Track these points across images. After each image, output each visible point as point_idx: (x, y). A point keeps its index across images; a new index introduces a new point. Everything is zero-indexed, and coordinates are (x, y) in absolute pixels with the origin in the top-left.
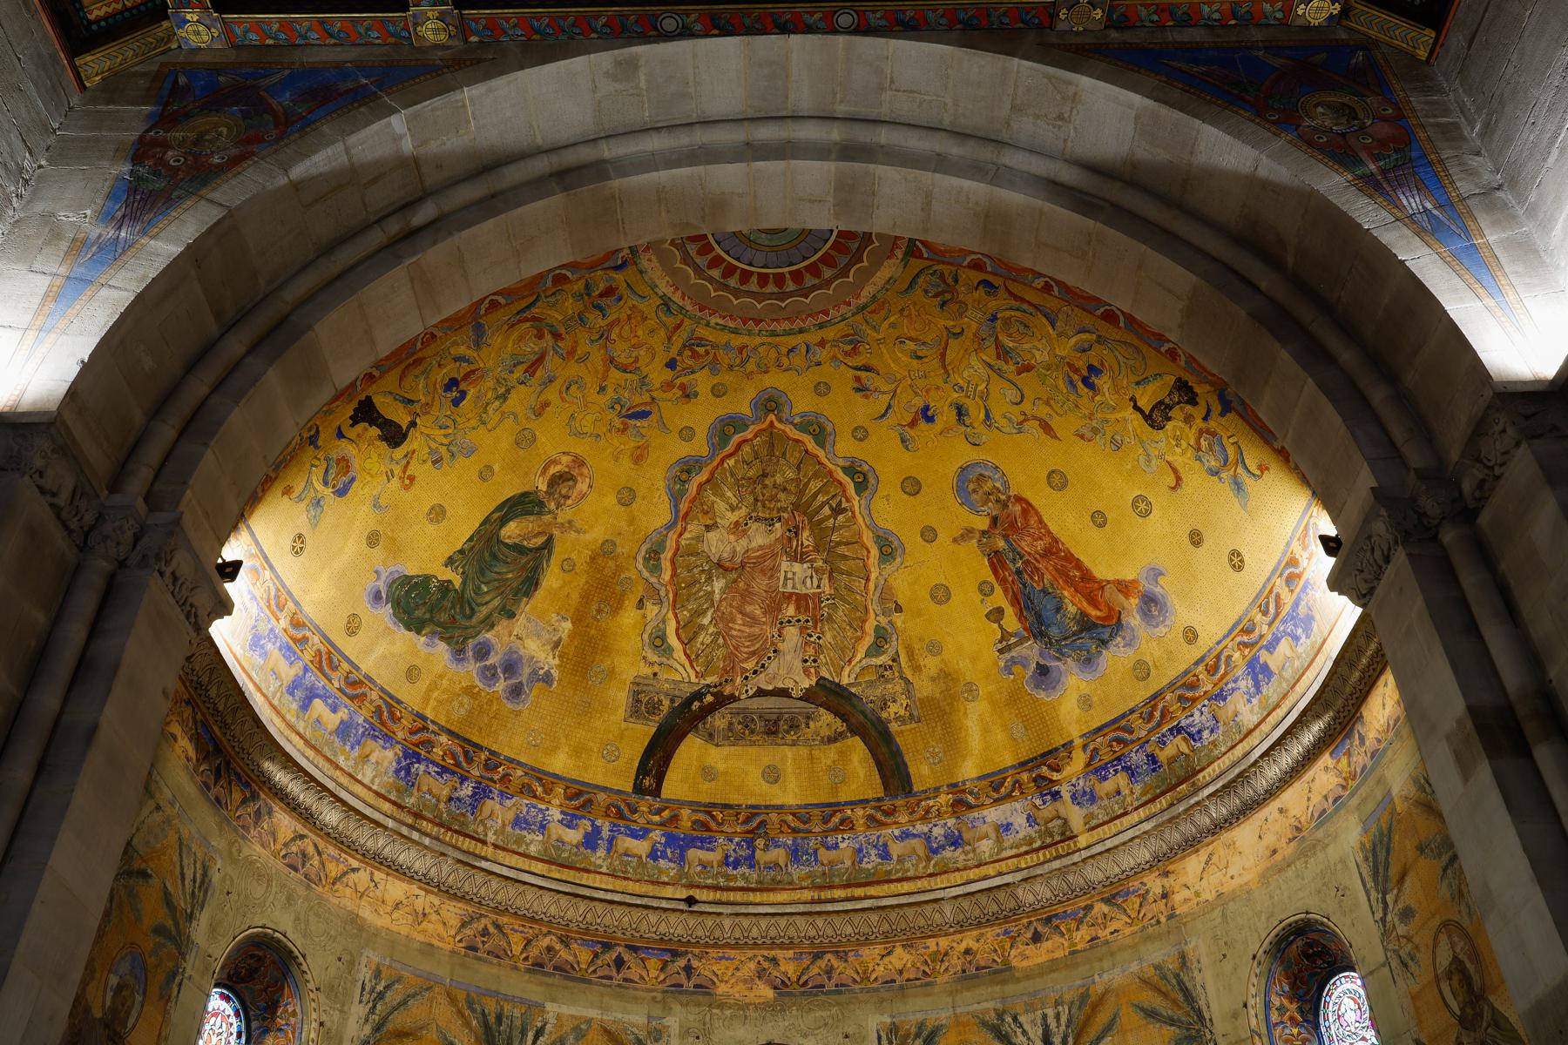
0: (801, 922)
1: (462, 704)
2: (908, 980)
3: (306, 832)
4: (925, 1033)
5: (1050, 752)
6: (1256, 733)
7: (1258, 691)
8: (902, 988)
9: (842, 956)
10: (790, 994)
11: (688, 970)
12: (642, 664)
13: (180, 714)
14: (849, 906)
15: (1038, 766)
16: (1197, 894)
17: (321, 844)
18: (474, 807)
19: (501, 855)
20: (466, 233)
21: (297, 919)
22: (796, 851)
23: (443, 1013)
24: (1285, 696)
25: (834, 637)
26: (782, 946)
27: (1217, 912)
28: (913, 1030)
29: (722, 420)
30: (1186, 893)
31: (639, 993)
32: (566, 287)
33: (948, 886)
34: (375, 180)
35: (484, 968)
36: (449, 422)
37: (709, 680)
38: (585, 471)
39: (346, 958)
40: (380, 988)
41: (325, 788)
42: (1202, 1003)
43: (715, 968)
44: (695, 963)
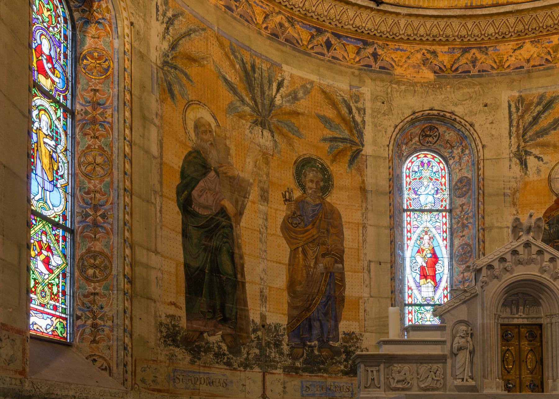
2: (533, 66)
4: (545, 102)
8: (528, 72)
9: (484, 50)
10: (445, 77)
11: (375, 55)
26: (440, 43)
28: (536, 100)
31: (343, 68)
43: (393, 56)
44: (380, 52)
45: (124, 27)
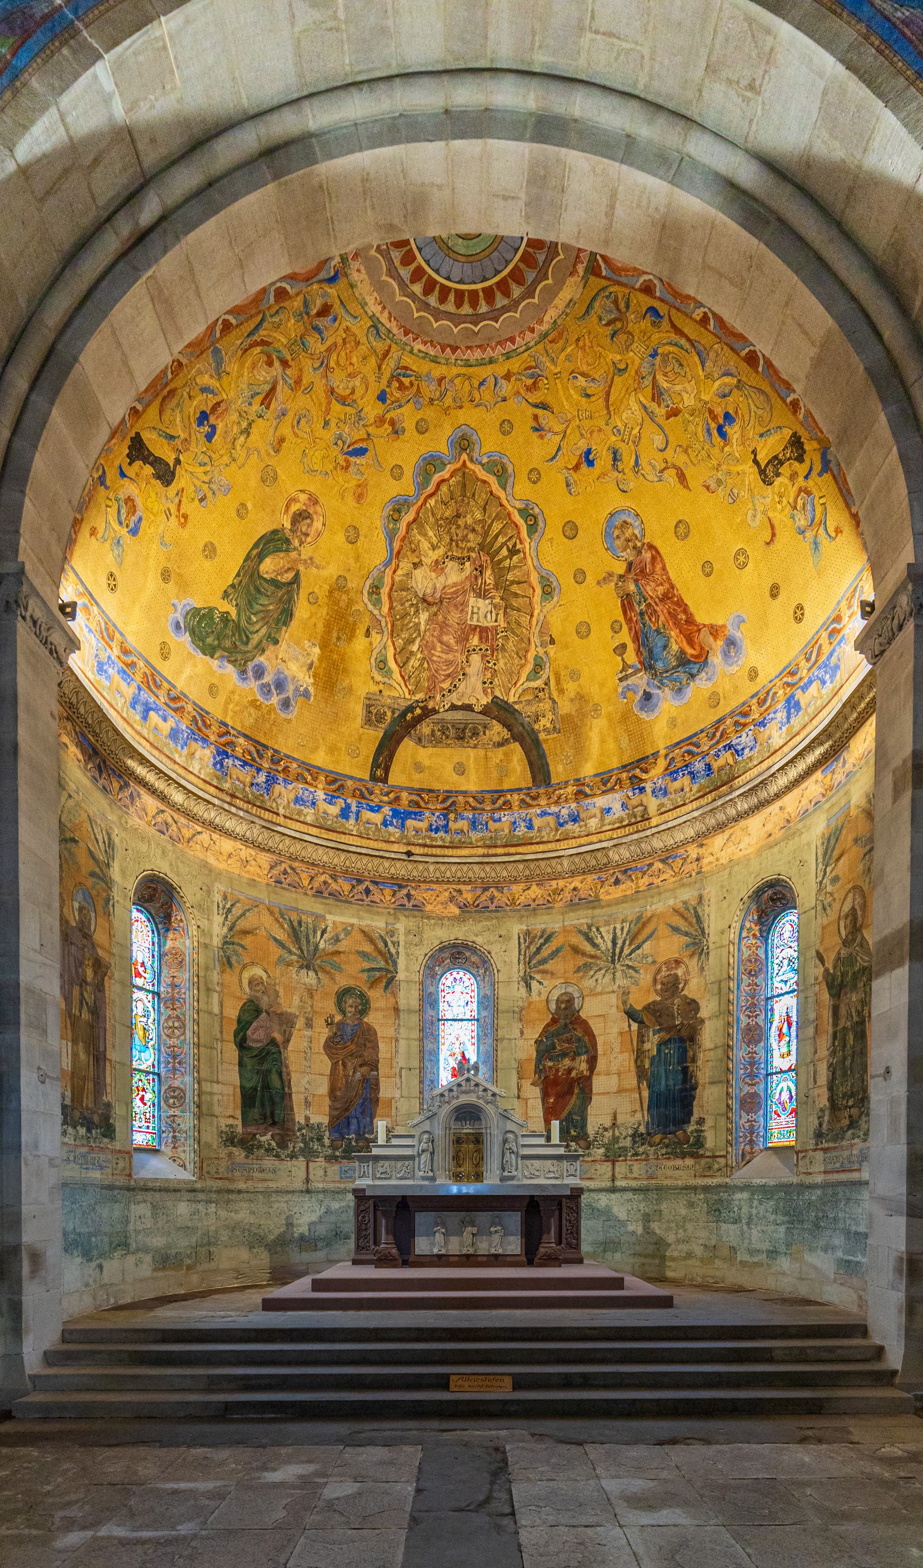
0: (476, 868)
1: (250, 715)
3: (164, 808)
5: (643, 759)
6: (779, 753)
7: (788, 721)
12: (371, 682)
13: (65, 728)
14: (506, 859)
15: (634, 769)
16: (717, 860)
17: (176, 817)
18: (268, 790)
19: (289, 823)
20: (192, 237)
21: (171, 865)
22: (474, 822)
23: (267, 920)
24: (804, 727)
25: (506, 664)
27: (727, 871)
29: (425, 459)
30: (711, 859)
32: (286, 304)
33: (567, 848)
34: (96, 161)
35: (287, 894)
36: (207, 460)
37: (419, 696)
38: (319, 509)
39: (204, 888)
40: (228, 906)
41: (170, 778)
42: (706, 925)
45: (193, 930)
